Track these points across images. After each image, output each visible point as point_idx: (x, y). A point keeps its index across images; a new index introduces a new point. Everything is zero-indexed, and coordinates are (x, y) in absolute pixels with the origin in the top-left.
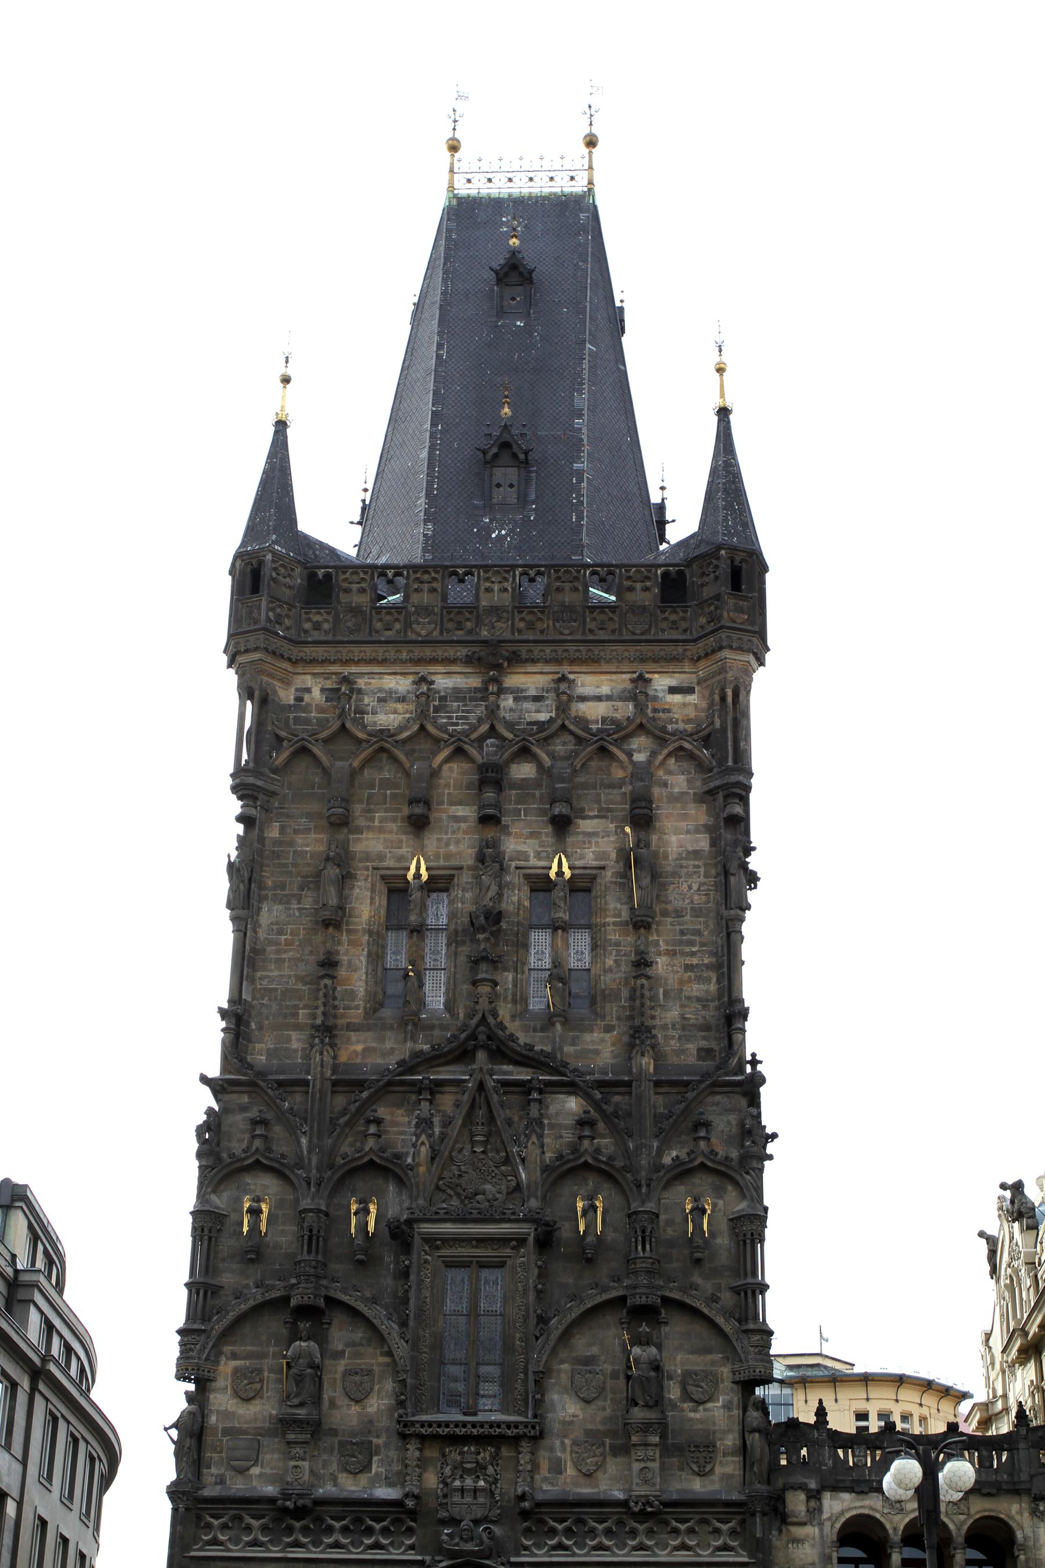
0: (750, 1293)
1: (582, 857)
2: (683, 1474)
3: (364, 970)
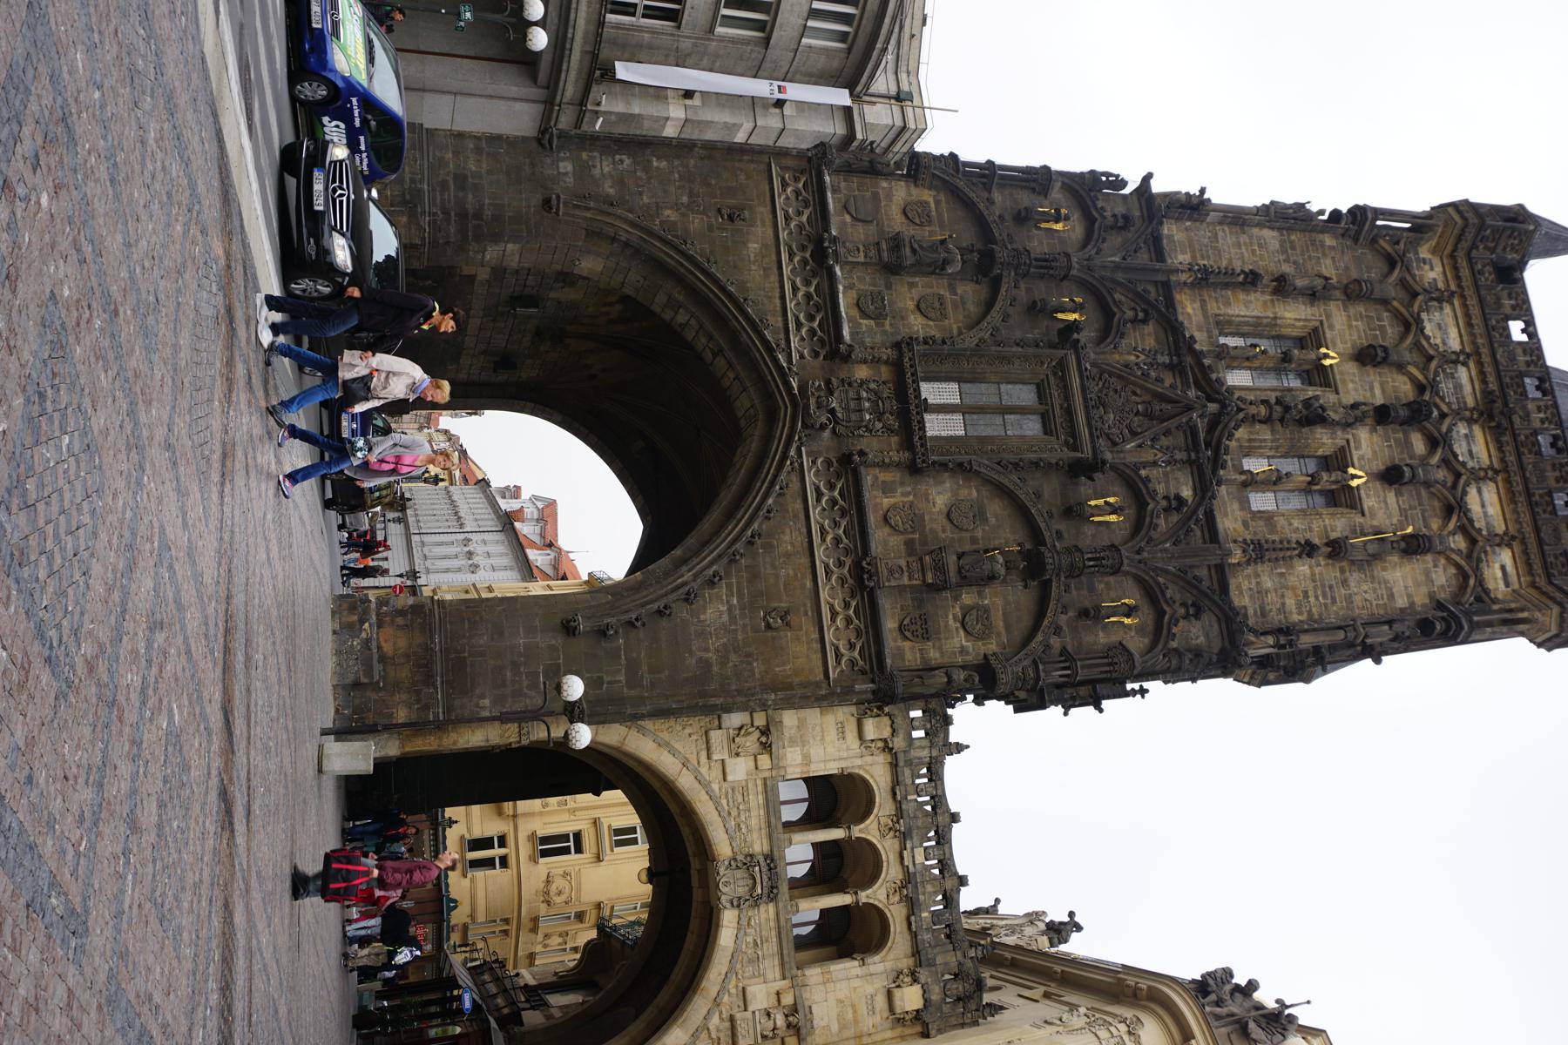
0: (1067, 664)
1: (1368, 496)
2: (898, 611)
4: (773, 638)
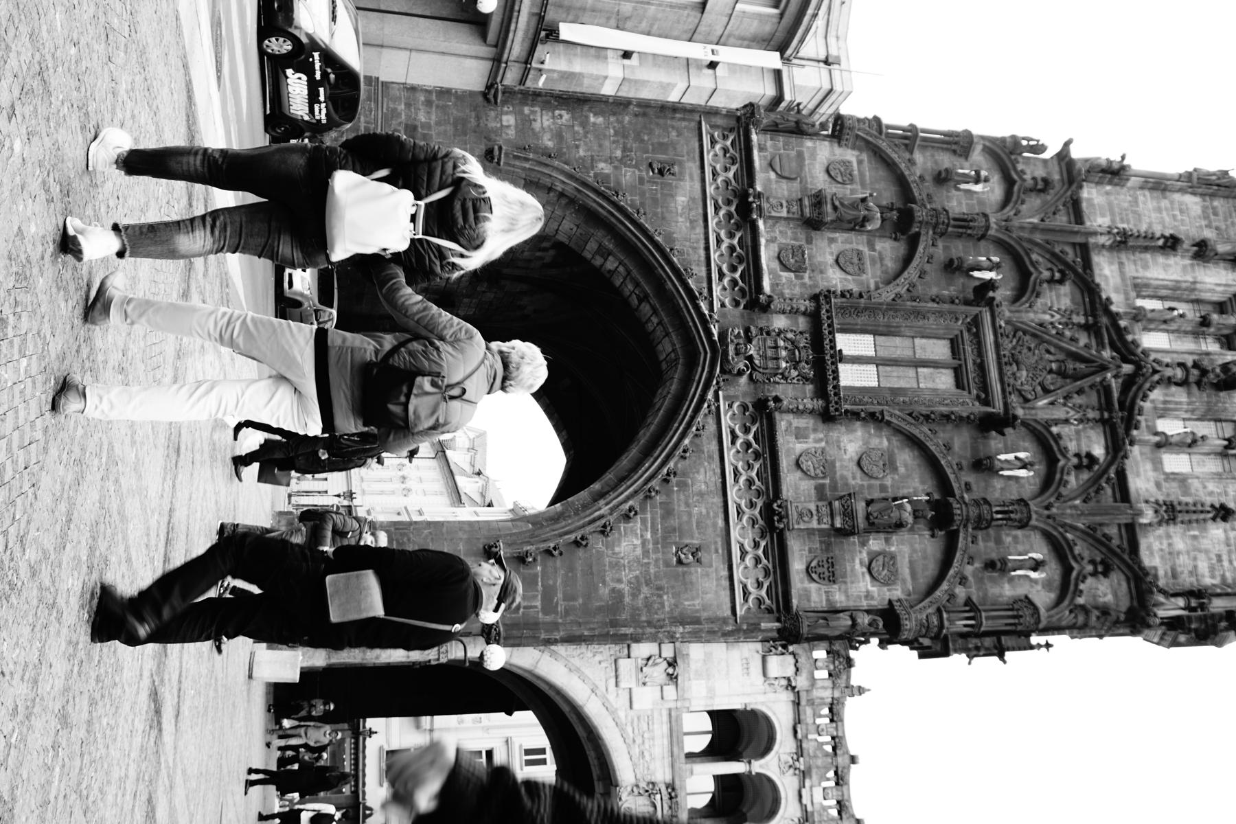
0: (971, 614)
2: (806, 553)
3: (1167, 277)
4: (684, 573)
